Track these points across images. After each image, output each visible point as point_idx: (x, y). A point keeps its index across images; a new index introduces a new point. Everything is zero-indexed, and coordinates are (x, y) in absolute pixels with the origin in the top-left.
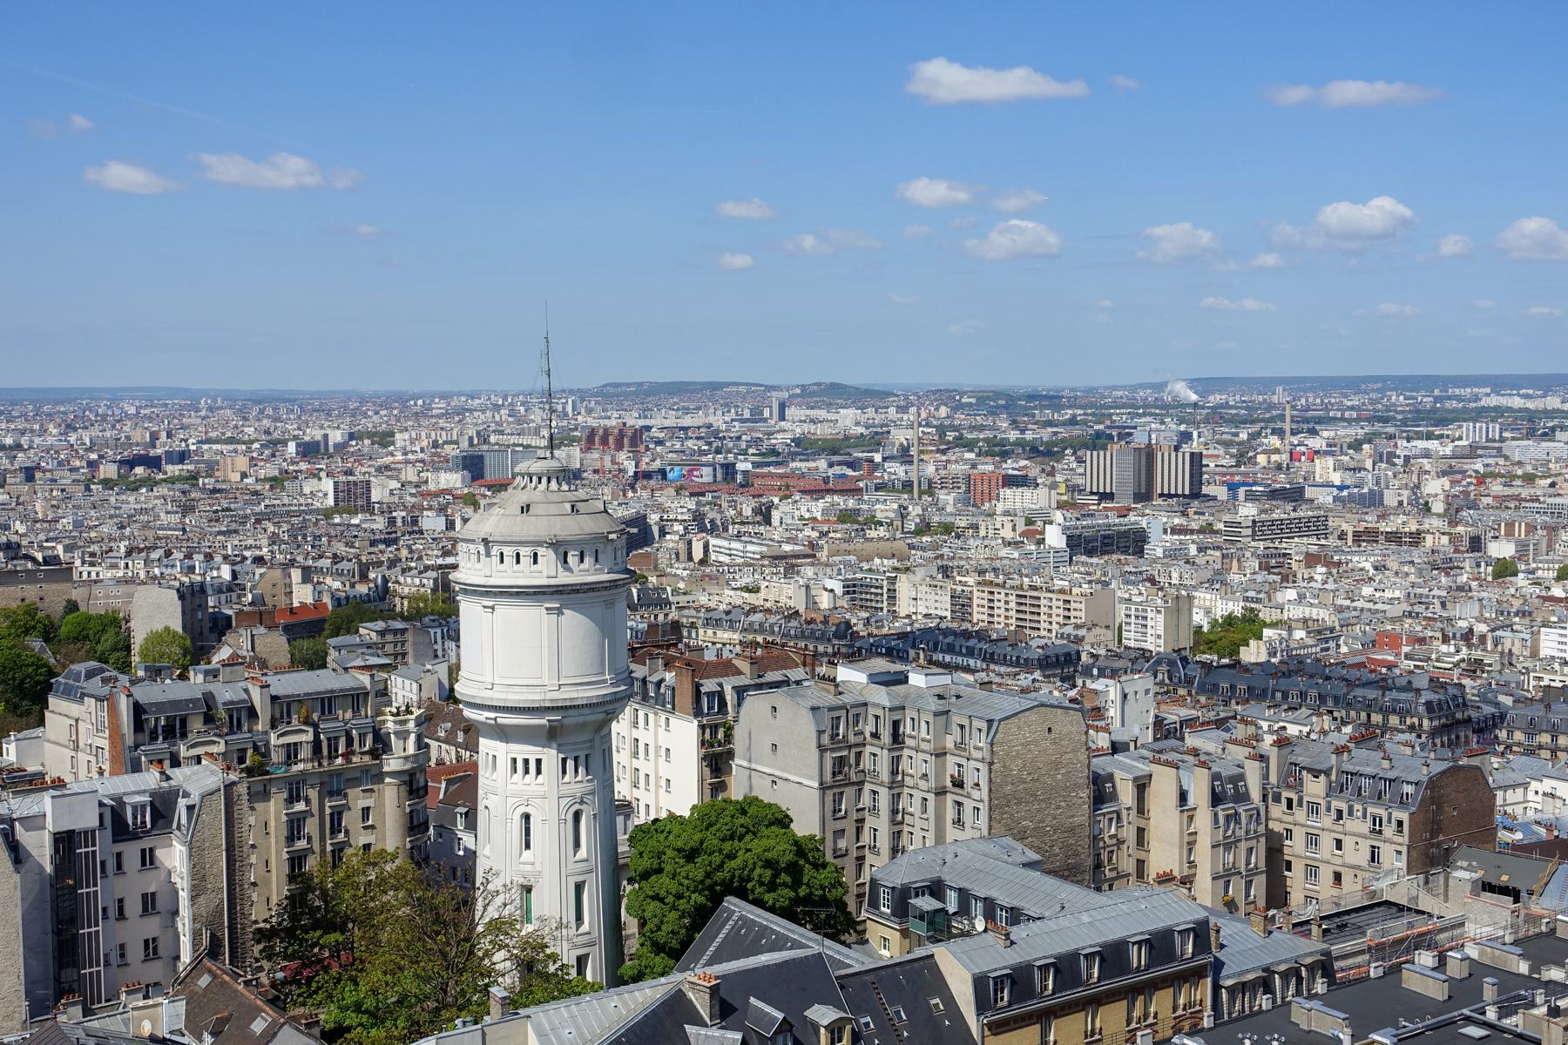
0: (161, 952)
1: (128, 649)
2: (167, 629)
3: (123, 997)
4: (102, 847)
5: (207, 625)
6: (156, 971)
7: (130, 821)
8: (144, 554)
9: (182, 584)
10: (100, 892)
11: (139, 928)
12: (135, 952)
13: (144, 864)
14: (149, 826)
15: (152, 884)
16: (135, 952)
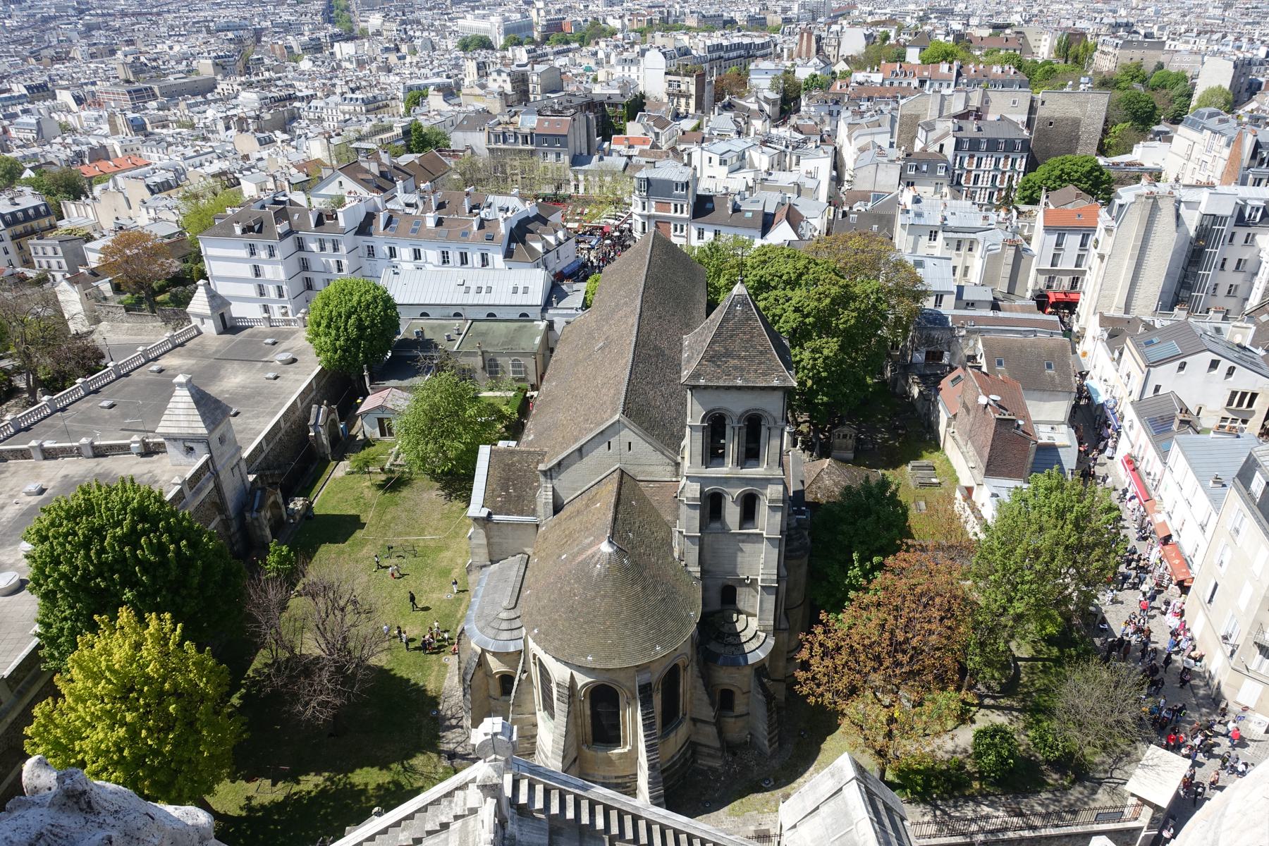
0: (1239, 293)
1: (1190, 96)
2: (1220, 87)
3: (1211, 313)
4: (1227, 229)
5: (1245, 86)
6: (1231, 304)
7: (1247, 215)
8: (1208, 35)
9: (1238, 58)
10: (1216, 252)
11: (1230, 277)
12: (1222, 290)
13: (1246, 242)
14: (1258, 220)
15: (1247, 254)
16: (1222, 290)
